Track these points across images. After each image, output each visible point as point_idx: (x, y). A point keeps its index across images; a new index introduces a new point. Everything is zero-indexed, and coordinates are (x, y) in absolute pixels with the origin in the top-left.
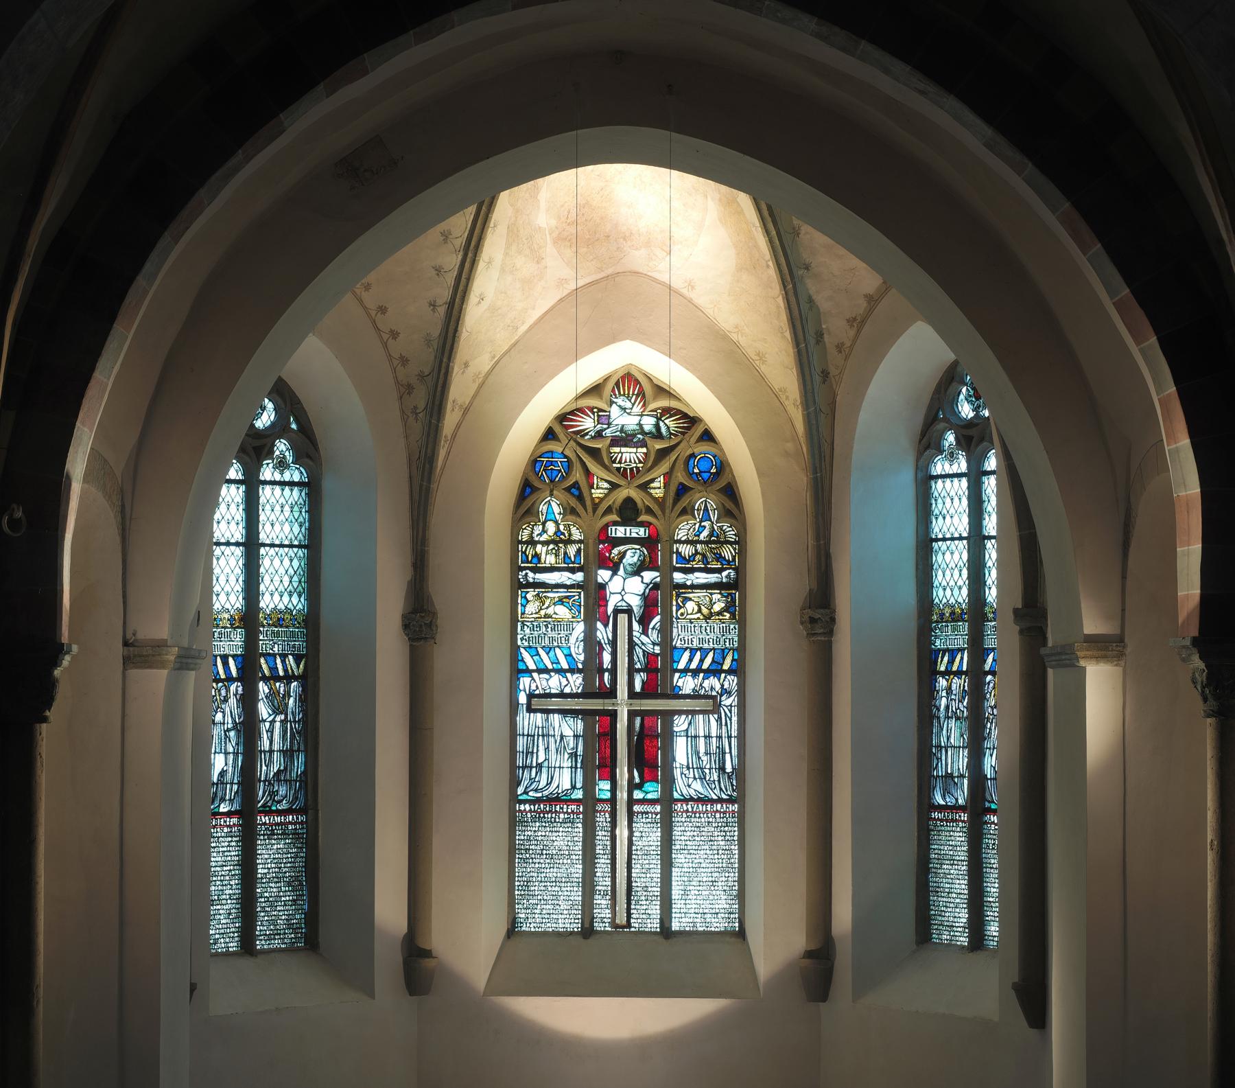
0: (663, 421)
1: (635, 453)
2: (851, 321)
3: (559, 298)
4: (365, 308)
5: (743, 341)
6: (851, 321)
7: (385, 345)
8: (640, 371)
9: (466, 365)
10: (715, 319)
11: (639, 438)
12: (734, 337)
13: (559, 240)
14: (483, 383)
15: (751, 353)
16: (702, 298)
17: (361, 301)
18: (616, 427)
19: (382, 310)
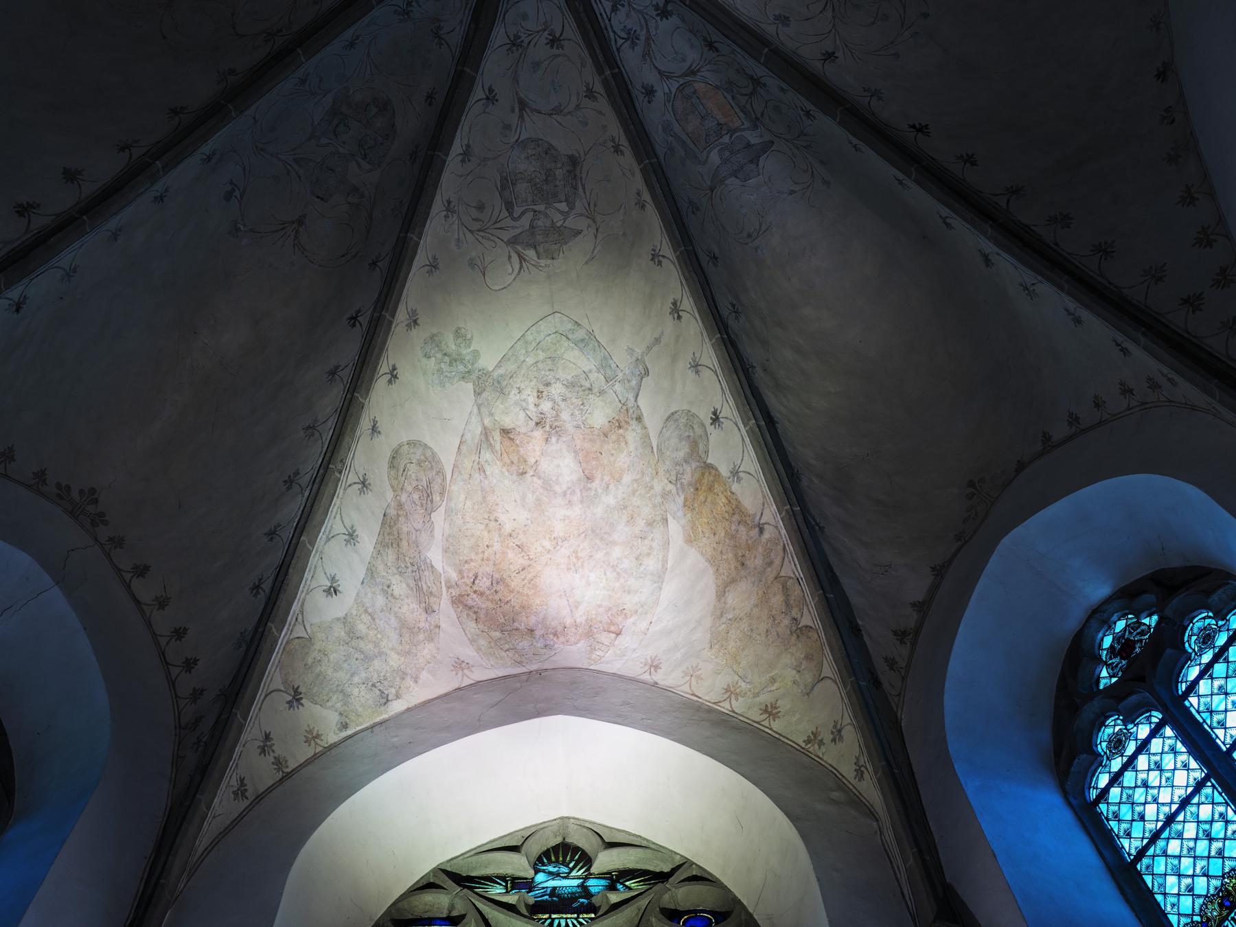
0: (621, 883)
1: (576, 919)
2: (901, 635)
3: (457, 686)
4: (154, 635)
5: (738, 706)
6: (901, 635)
7: (172, 683)
8: (582, 825)
9: (296, 698)
10: (693, 695)
11: (583, 903)
12: (725, 707)
13: (458, 601)
14: (322, 754)
15: (755, 715)
16: (665, 678)
17: (149, 624)
18: (545, 890)
19: (179, 633)
